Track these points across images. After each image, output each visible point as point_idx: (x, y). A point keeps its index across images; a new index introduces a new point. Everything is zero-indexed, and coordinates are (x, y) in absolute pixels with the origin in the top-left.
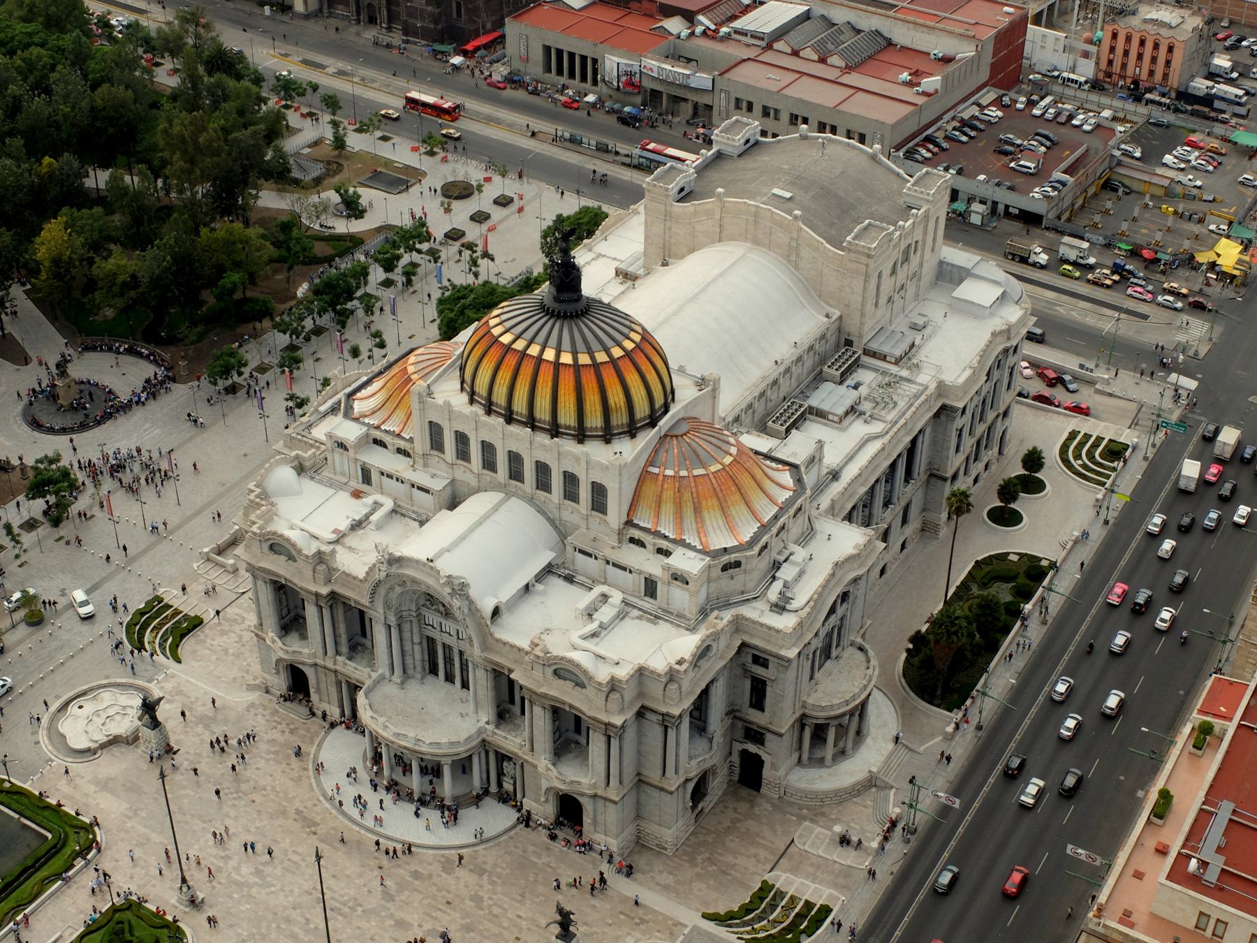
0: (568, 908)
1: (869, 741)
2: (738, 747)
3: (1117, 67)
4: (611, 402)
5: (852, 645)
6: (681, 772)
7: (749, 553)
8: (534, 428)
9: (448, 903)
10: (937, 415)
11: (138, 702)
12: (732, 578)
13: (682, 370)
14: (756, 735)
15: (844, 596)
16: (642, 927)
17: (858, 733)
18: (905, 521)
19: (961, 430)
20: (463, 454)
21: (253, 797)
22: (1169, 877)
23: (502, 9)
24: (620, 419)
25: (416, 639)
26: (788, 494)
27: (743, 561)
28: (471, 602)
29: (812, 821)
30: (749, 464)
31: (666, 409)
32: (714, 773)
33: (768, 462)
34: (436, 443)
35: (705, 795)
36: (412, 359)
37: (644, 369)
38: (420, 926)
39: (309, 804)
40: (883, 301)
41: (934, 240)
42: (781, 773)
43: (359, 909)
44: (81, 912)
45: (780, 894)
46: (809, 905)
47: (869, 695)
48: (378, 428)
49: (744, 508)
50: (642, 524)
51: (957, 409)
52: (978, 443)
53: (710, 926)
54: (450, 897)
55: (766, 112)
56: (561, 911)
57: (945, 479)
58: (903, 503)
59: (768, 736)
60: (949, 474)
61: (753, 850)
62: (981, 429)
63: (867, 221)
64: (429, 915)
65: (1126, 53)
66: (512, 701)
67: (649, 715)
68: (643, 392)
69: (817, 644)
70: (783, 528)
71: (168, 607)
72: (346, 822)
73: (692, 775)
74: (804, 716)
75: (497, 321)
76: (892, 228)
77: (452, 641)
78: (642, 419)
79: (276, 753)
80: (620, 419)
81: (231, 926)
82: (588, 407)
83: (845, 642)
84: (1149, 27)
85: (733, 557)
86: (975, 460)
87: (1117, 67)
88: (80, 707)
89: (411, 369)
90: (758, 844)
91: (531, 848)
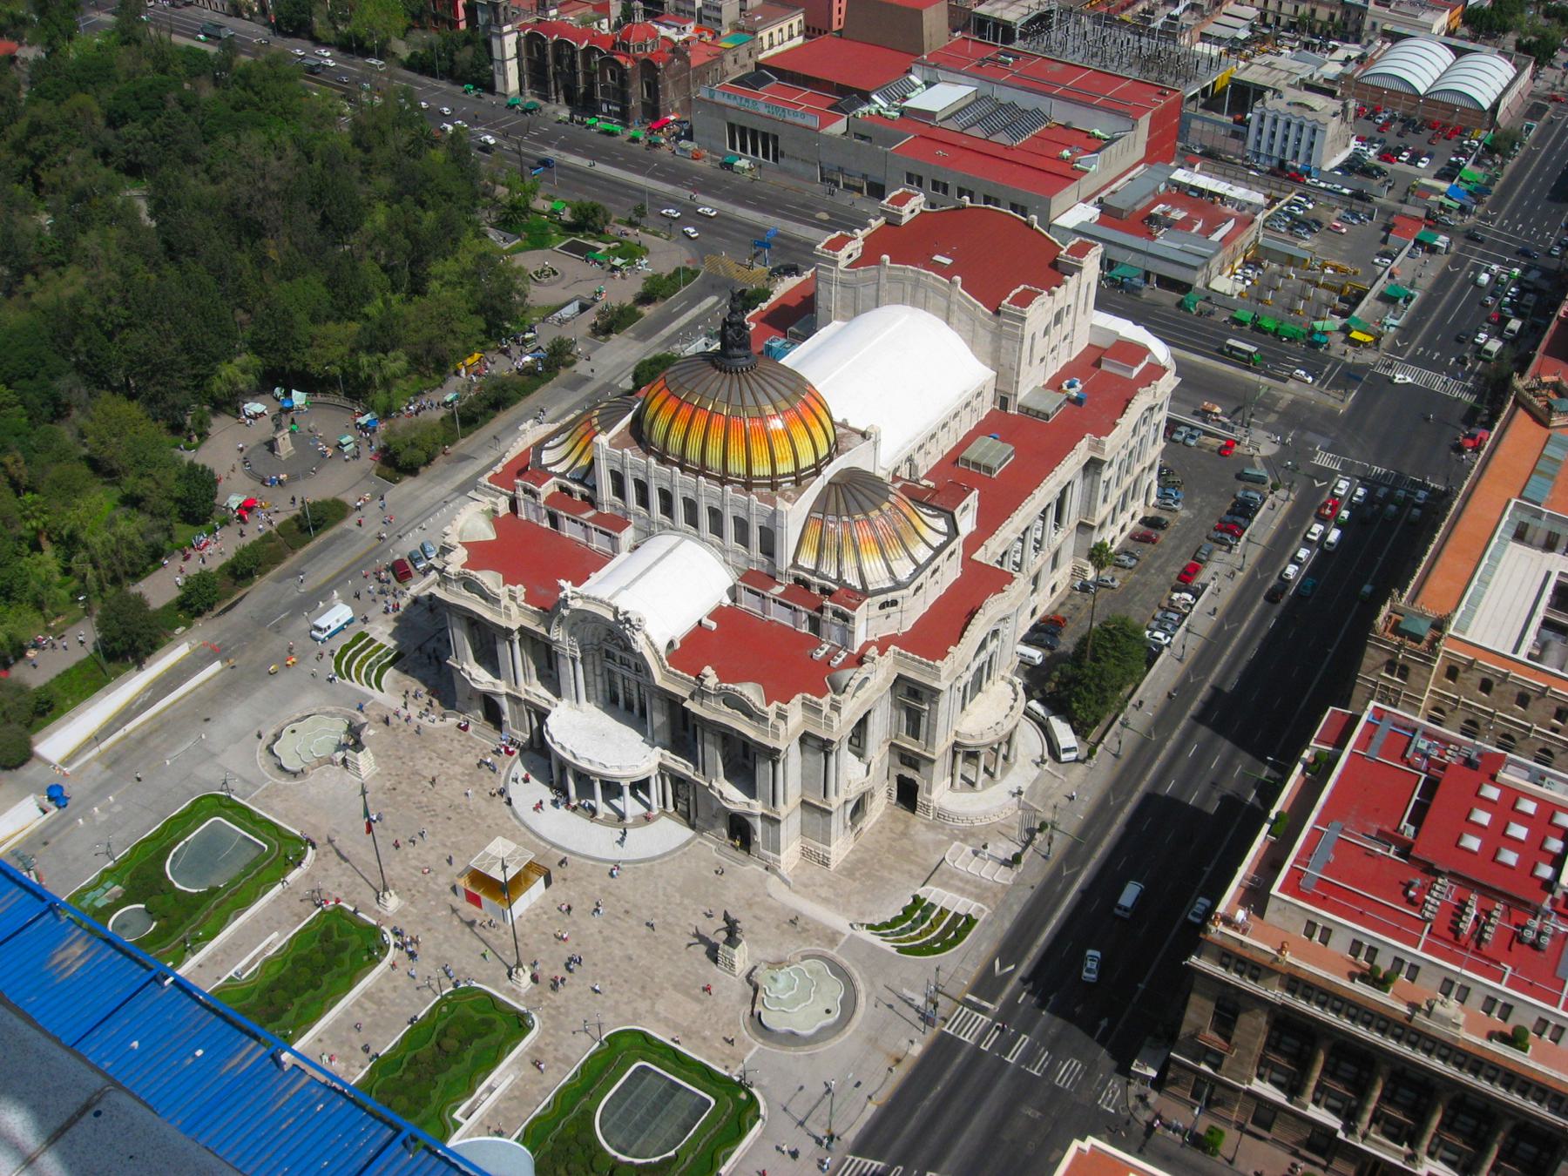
0: (733, 916)
1: (1016, 768)
2: (894, 773)
3: (1263, 149)
4: (778, 454)
5: (1003, 678)
6: (841, 793)
7: (904, 592)
8: (707, 476)
9: (627, 912)
10: (1086, 468)
11: (345, 727)
12: (888, 617)
13: (844, 425)
14: (910, 760)
15: (995, 633)
16: (804, 935)
17: (1006, 758)
18: (1054, 565)
19: (1108, 483)
20: (644, 501)
21: (449, 814)
22: (1282, 889)
23: (689, 89)
24: (786, 467)
25: (598, 672)
26: (943, 539)
27: (900, 600)
28: (648, 637)
29: (962, 840)
30: (906, 510)
31: (830, 458)
32: (872, 796)
33: (925, 510)
34: (619, 490)
35: (864, 814)
36: (597, 412)
37: (808, 422)
38: (600, 932)
39: (500, 822)
40: (1036, 361)
41: (1086, 304)
42: (934, 796)
43: (545, 917)
44: (296, 915)
45: (933, 906)
46: (957, 916)
47: (1016, 726)
48: (562, 475)
49: (902, 553)
50: (806, 566)
51: (1104, 462)
52: (1125, 495)
53: (866, 935)
54: (627, 906)
55: (936, 185)
56: (726, 918)
57: (1092, 528)
58: (1053, 550)
59: (922, 762)
60: (1096, 523)
61: (907, 867)
62: (1128, 481)
63: (1022, 287)
64: (609, 923)
65: (1273, 135)
66: (686, 728)
67: (810, 741)
68: (808, 442)
69: (968, 677)
70: (935, 572)
71: (372, 641)
72: (532, 837)
73: (851, 797)
74: (956, 744)
75: (673, 376)
76: (1045, 293)
77: (626, 674)
78: (807, 469)
79: (470, 775)
80: (786, 467)
81: (429, 930)
82: (755, 456)
83: (995, 676)
84: (1295, 110)
85: (890, 596)
86: (1122, 510)
87: (1263, 149)
88: (293, 731)
89: (595, 421)
90: (913, 862)
91: (703, 864)
